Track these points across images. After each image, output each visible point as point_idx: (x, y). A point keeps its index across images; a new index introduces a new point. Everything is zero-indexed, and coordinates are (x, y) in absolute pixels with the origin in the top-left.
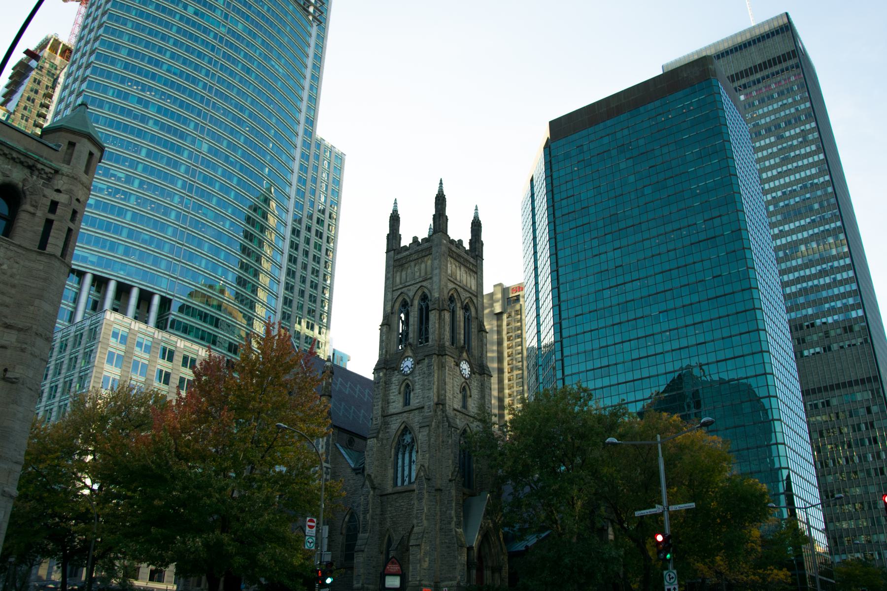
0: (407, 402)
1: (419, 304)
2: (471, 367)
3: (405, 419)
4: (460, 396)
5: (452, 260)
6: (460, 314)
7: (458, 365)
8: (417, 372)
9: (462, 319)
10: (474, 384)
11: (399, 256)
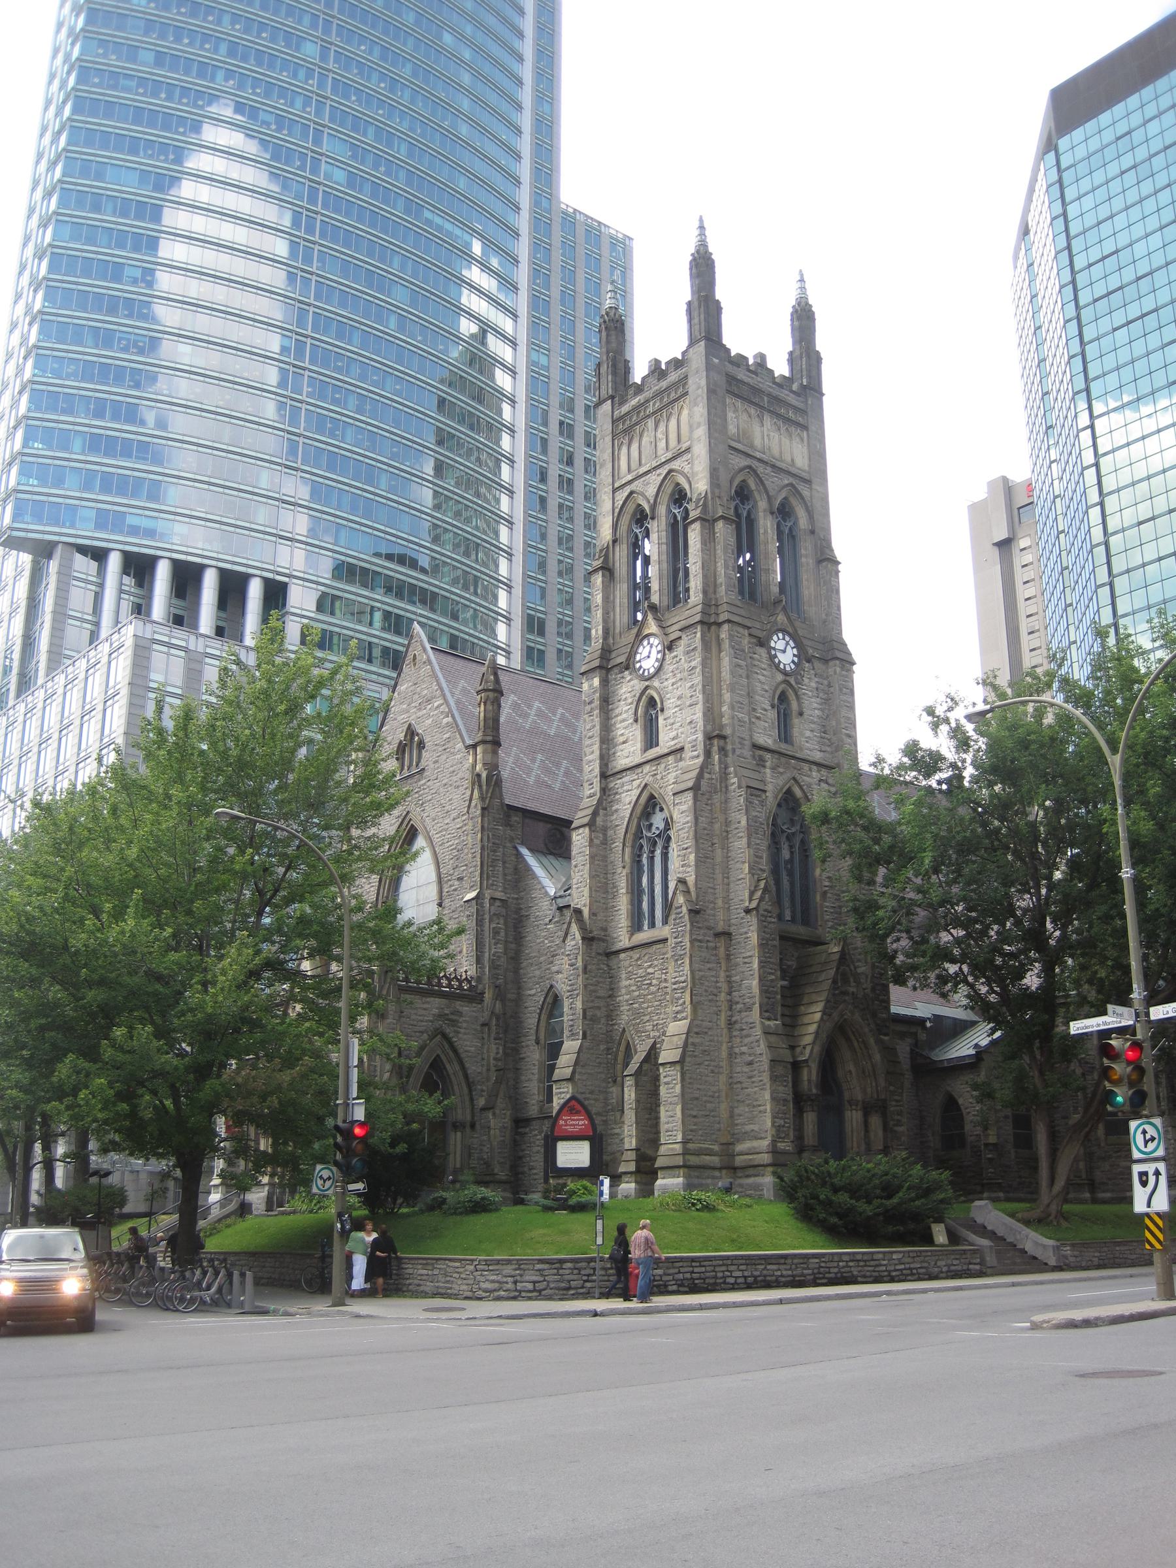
0: (651, 739)
1: (669, 511)
2: (799, 645)
3: (648, 779)
4: (772, 714)
5: (739, 403)
7: (763, 643)
8: (668, 668)
10: (809, 683)
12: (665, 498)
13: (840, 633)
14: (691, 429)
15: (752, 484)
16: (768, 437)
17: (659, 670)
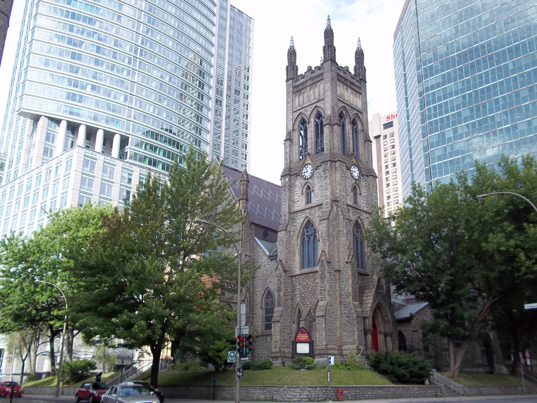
0: (309, 201)
2: (359, 170)
6: (348, 127)
9: (351, 131)
10: (363, 184)
11: (298, 83)
12: (313, 116)
13: (372, 166)
14: (324, 92)
15: (344, 112)
16: (349, 96)
17: (311, 177)
